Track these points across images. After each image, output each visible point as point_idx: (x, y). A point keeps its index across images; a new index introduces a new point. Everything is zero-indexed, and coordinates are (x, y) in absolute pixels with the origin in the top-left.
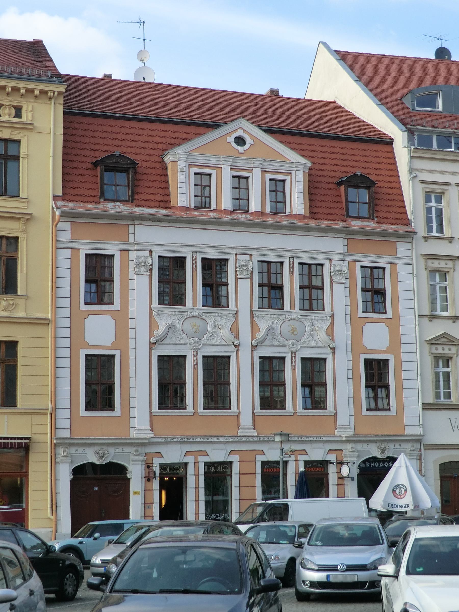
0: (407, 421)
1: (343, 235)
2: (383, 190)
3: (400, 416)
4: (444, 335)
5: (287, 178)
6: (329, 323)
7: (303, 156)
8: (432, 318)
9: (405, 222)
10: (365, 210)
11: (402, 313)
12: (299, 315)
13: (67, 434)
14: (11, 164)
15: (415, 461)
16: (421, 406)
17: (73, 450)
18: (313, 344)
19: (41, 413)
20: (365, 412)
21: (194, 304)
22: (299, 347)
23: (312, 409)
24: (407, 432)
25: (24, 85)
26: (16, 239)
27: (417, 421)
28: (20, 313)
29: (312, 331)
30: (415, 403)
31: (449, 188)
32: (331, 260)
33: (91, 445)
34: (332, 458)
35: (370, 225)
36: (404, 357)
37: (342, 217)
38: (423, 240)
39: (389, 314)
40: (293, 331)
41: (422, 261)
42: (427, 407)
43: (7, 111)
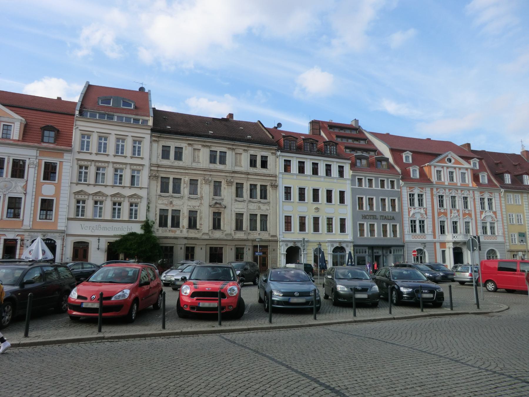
0: (59, 224)
1: (37, 149)
2: (64, 133)
3: (56, 223)
4: (81, 191)
5: (12, 125)
6: (25, 183)
7: (21, 116)
8: (77, 184)
9: (70, 145)
10: (52, 140)
11: (63, 181)
12: (9, 179)
15: (60, 241)
16: (67, 219)
18: (15, 191)
20: (38, 220)
21: (7, 176)
22: (8, 193)
23: (14, 218)
24: (58, 229)
27: (64, 225)
29: (15, 186)
30: (64, 217)
31: (93, 133)
32: (29, 158)
34: (19, 238)
35: (52, 146)
36: (61, 199)
37: (39, 142)
38: (130, 158)
39: (56, 182)
40: (5, 186)
41: (76, 161)
42: (69, 219)
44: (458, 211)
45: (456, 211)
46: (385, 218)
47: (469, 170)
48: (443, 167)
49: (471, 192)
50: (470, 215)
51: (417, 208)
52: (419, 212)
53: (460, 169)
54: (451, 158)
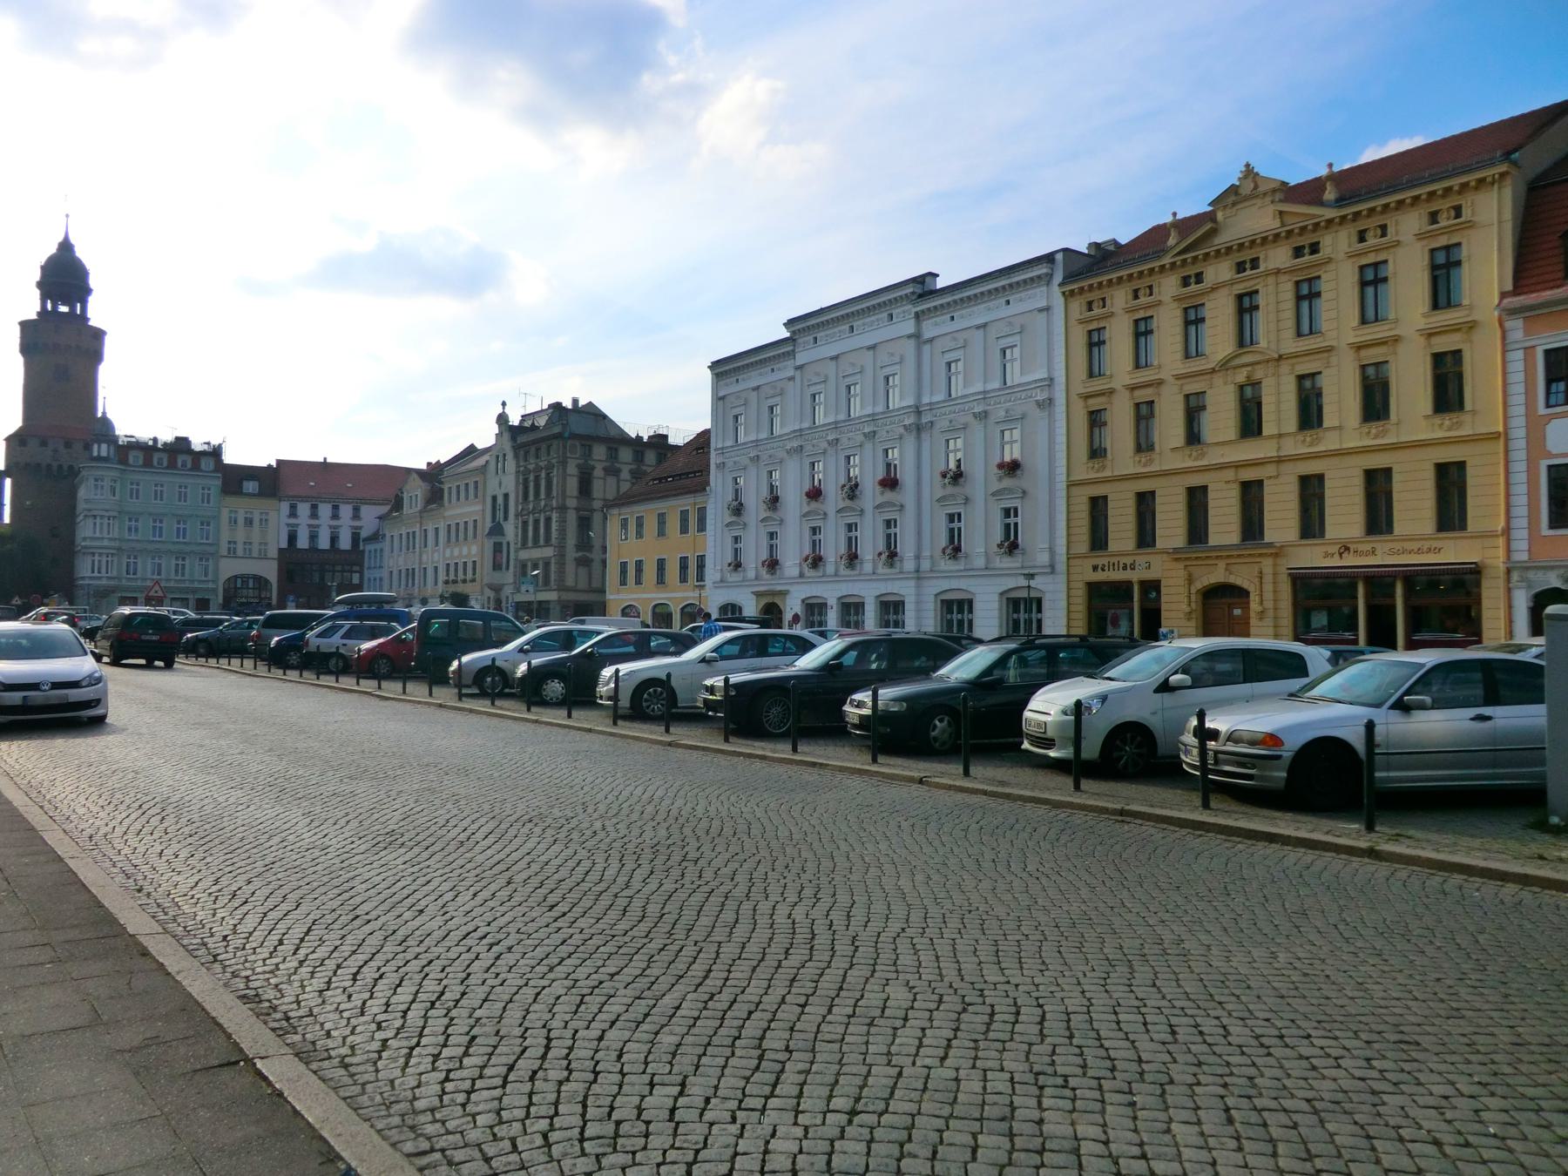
13: (1524, 557)
14: (1453, 272)
17: (1531, 575)
19: (1493, 535)
25: (1455, 182)
26: (1459, 352)
28: (1466, 431)
33: (1552, 568)
43: (1445, 215)
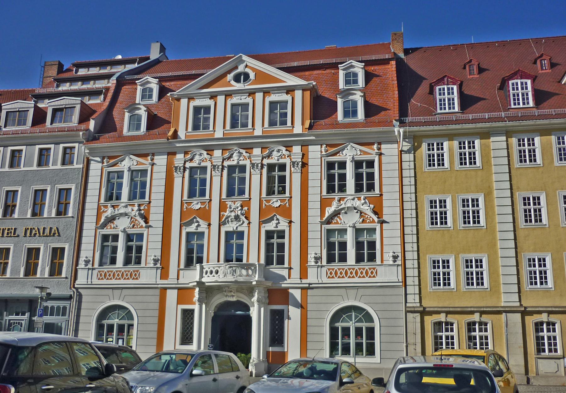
44: (247, 203)
45: (238, 204)
46: (30, 233)
47: (298, 94)
48: (213, 96)
49: (297, 149)
50: (286, 211)
51: (123, 205)
52: (126, 214)
53: (266, 92)
54: (247, 70)
